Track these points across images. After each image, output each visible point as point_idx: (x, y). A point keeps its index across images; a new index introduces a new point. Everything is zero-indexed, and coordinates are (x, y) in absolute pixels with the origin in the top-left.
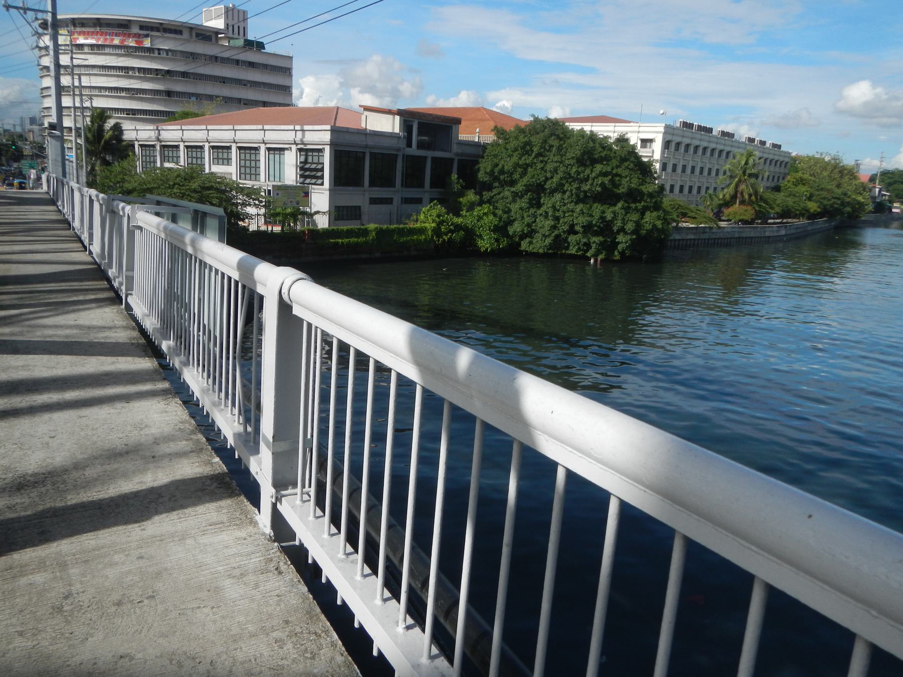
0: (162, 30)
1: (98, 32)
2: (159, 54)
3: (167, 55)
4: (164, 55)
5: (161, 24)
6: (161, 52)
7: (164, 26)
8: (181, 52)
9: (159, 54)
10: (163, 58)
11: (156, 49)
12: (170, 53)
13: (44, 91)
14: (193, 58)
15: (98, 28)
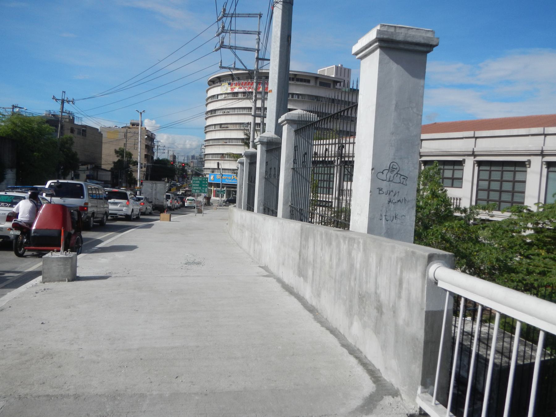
0: (295, 79)
1: (249, 83)
2: (292, 97)
3: (298, 98)
4: (295, 98)
5: (295, 75)
6: (294, 96)
7: (297, 77)
8: (308, 95)
9: (292, 97)
10: (295, 101)
11: (291, 94)
12: (300, 97)
13: (207, 128)
14: (317, 100)
15: (250, 80)
